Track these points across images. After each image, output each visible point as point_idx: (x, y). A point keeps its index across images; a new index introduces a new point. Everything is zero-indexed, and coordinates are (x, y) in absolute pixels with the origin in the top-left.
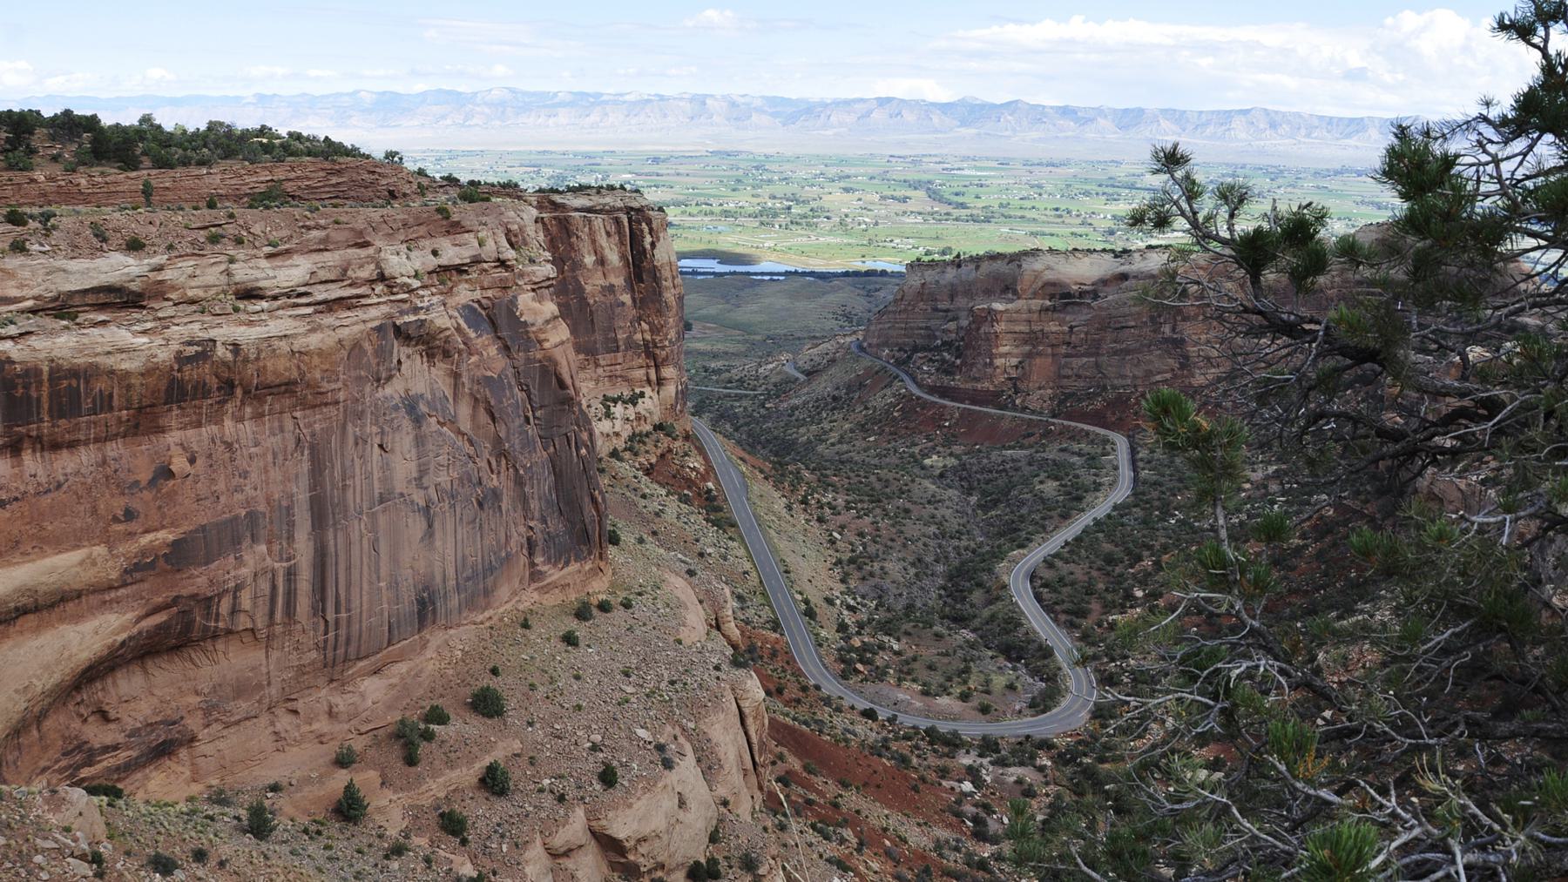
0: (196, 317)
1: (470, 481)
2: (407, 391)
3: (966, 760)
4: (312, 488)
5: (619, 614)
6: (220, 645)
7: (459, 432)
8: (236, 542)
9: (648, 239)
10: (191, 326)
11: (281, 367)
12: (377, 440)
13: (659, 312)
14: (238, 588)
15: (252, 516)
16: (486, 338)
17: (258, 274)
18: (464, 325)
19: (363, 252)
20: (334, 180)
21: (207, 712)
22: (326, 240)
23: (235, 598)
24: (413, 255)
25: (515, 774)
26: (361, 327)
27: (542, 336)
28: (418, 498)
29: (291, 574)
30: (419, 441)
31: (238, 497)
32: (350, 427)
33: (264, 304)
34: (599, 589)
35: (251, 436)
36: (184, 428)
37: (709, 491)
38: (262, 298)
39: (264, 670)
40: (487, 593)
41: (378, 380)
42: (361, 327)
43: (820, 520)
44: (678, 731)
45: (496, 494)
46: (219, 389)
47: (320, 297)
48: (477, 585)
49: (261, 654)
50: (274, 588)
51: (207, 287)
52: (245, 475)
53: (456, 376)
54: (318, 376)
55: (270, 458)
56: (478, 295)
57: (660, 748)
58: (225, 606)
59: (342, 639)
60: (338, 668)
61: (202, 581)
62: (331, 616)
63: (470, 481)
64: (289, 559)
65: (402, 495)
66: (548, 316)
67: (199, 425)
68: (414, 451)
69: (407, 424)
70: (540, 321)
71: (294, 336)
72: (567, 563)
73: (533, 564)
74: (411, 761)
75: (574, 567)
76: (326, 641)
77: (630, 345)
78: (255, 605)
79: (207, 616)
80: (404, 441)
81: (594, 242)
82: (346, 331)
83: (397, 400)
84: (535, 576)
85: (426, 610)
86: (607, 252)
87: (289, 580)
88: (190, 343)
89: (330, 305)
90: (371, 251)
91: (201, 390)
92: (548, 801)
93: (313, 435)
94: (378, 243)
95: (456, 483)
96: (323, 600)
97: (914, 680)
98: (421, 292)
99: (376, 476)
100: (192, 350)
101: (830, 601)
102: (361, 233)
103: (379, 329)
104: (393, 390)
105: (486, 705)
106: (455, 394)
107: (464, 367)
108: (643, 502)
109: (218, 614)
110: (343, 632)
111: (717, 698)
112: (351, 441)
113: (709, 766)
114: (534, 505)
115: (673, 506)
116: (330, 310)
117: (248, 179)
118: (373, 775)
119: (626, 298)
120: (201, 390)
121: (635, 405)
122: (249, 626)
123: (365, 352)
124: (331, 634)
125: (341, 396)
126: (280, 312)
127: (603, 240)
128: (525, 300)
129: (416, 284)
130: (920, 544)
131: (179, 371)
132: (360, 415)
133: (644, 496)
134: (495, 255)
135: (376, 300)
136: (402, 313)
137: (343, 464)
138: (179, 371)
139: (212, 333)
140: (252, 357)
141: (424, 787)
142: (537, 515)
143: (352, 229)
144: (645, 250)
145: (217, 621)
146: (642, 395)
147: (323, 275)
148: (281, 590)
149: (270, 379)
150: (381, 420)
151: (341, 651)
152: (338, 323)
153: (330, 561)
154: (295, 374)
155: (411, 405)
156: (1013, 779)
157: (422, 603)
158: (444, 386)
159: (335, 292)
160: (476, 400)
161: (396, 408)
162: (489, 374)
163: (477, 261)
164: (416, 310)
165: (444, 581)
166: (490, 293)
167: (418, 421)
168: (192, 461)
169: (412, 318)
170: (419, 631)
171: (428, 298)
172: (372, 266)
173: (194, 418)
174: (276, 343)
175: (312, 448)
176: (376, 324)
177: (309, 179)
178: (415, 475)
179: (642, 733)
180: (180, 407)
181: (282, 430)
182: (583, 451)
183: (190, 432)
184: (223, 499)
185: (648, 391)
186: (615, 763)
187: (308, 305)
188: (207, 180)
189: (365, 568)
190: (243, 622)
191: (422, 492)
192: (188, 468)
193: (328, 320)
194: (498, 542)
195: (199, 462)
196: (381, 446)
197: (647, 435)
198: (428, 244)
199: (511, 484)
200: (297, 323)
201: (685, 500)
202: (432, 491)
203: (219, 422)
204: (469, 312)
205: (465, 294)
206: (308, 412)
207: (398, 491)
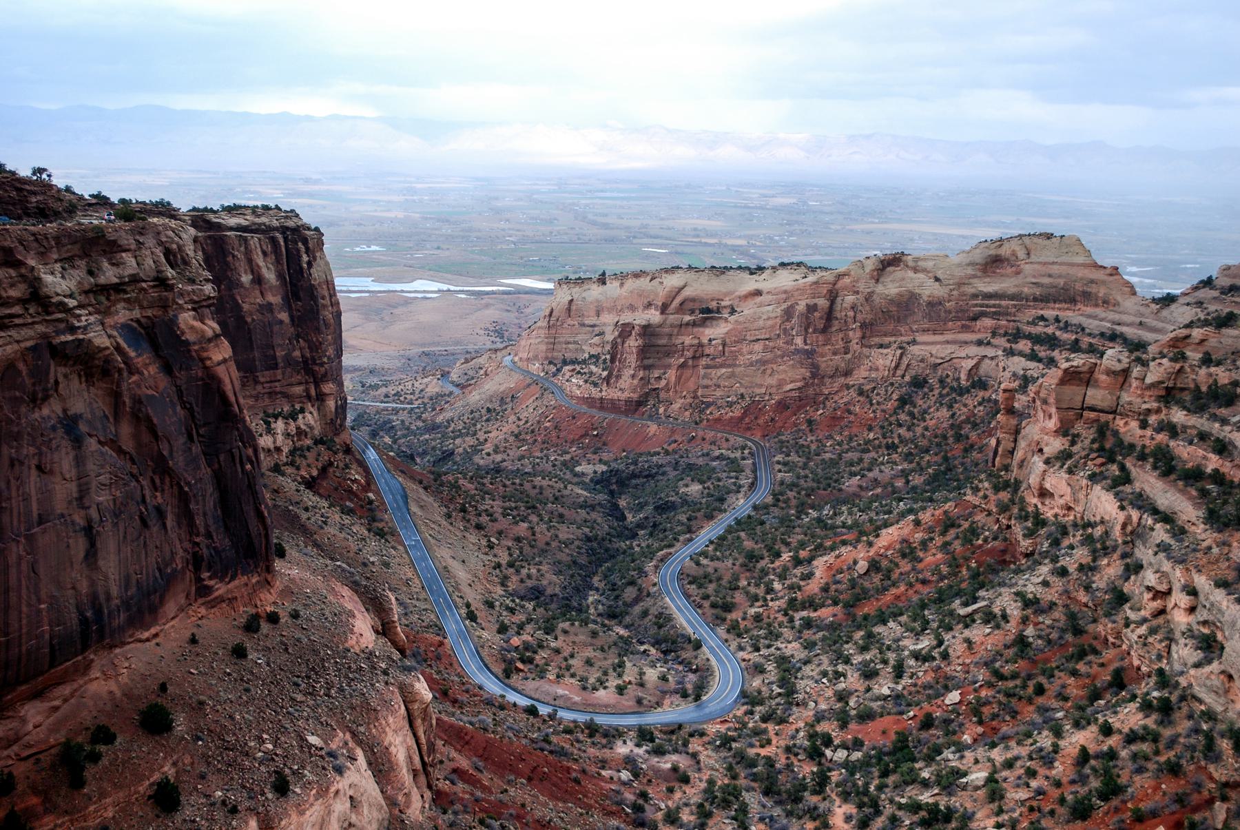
2: (65, 411)
3: (623, 749)
9: (305, 258)
12: (34, 462)
13: (318, 330)
26: (16, 347)
27: (205, 355)
30: (79, 461)
37: (371, 502)
42: (16, 347)
43: (479, 527)
44: (348, 736)
56: (137, 313)
57: (331, 754)
72: (233, 578)
73: (199, 580)
77: (289, 361)
80: (64, 461)
81: (250, 261)
86: (264, 271)
97: (573, 676)
98: (78, 312)
99: (34, 499)
103: (33, 349)
104: (50, 411)
107: (124, 386)
111: (387, 703)
113: (381, 768)
114: (199, 521)
115: (335, 516)
119: (284, 316)
121: (295, 420)
123: (20, 372)
130: (572, 547)
133: (307, 509)
134: (154, 274)
135: (30, 321)
136: (58, 333)
142: (202, 530)
144: (301, 268)
146: (302, 411)
150: (39, 440)
156: (669, 766)
157: (84, 621)
158: (102, 406)
161: (54, 428)
166: (149, 313)
167: (77, 442)
169: (70, 338)
171: (86, 318)
176: (29, 344)
178: (75, 495)
179: (313, 740)
186: (287, 771)
191: (83, 512)
196: (39, 468)
197: (309, 449)
202: (94, 513)
205: (123, 315)
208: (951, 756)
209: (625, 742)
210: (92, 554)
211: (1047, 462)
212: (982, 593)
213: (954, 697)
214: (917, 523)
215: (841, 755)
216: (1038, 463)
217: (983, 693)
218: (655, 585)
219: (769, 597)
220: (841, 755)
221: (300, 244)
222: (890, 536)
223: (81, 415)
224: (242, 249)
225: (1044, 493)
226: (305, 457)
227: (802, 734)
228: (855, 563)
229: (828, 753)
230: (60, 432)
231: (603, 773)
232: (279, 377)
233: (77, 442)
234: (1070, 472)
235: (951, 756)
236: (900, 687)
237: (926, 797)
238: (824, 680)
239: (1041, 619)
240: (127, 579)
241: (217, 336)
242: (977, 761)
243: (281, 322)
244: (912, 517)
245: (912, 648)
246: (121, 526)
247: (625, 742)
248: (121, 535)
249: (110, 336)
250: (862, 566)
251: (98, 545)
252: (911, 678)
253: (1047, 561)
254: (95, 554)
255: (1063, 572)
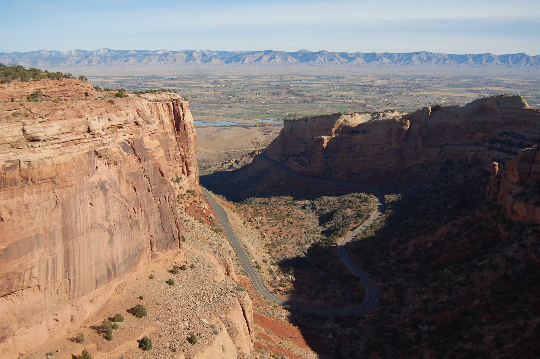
0: (12, 150)
1: (127, 217)
2: (100, 180)
3: (329, 325)
4: (63, 223)
5: (189, 271)
6: (24, 292)
7: (121, 196)
8: (31, 248)
9: (181, 113)
10: (8, 154)
11: (48, 171)
12: (89, 201)
13: (187, 143)
14: (32, 268)
15: (37, 236)
16: (132, 156)
17: (37, 130)
18: (122, 151)
19: (80, 120)
20: (62, 89)
21: (19, 323)
22: (64, 115)
23: (31, 272)
24: (100, 120)
25: (154, 342)
26: (81, 152)
27: (154, 154)
28: (106, 225)
29: (54, 261)
30: (106, 201)
31: (31, 228)
32: (78, 197)
33: (41, 144)
34: (180, 261)
35: (36, 201)
36: (7, 199)
37: (211, 218)
38: (39, 141)
39: (43, 303)
40: (135, 264)
41: (89, 175)
42: (81, 152)
43: (257, 228)
44: (219, 319)
45: (137, 222)
46: (22, 181)
47: (64, 140)
48: (131, 262)
49: (42, 296)
50: (48, 267)
51: (14, 137)
52: (33, 218)
53: (120, 172)
54: (64, 174)
55: (44, 210)
56: (127, 137)
57: (212, 327)
58: (27, 276)
59: (77, 288)
60: (75, 299)
61: (17, 265)
62: (72, 278)
63: (127, 217)
64: (54, 254)
65: (100, 224)
66: (156, 146)
67: (13, 197)
68: (104, 205)
69: (101, 194)
70: (153, 148)
71: (54, 157)
72: (166, 250)
73: (152, 251)
74: (108, 338)
75: (169, 252)
76: (70, 289)
77: (175, 158)
78: (40, 275)
79: (19, 281)
80: (99, 201)
81: (159, 114)
82: (75, 154)
83: (97, 183)
84: (154, 256)
85: (111, 272)
86: (164, 118)
87: (54, 263)
88: (8, 162)
89: (66, 143)
90: (83, 119)
91: (14, 182)
92: (169, 352)
93: (63, 200)
94: (87, 116)
95: (121, 218)
96: (68, 271)
97: (304, 293)
98: (105, 137)
99: (89, 217)
100: (9, 165)
101: (265, 261)
102: (79, 112)
103: (89, 153)
104: (95, 179)
105: (137, 312)
106: (119, 181)
107: (123, 168)
108: (185, 223)
109: (24, 280)
110: (77, 284)
111: (233, 304)
112: (78, 202)
113: (232, 333)
114: (152, 226)
115: (197, 224)
116: (68, 145)
117: (26, 89)
118: (93, 345)
119: (173, 138)
120: (14, 182)
121: (178, 182)
122: (37, 284)
123: (83, 163)
124: (72, 286)
125: (74, 182)
126: (47, 147)
127: (162, 113)
128: (146, 139)
129: (103, 133)
130: (299, 236)
131: (4, 174)
132: (82, 191)
133: (185, 221)
134: (134, 120)
135: (87, 141)
136: (98, 146)
137: (75, 212)
138: (4, 174)
139: (19, 157)
140: (36, 167)
141: (116, 349)
142: (154, 231)
143: (76, 110)
144: (180, 117)
145: (23, 282)
146: (181, 178)
147: (64, 130)
148: (50, 268)
149: (44, 176)
150: (90, 192)
151: (76, 293)
152: (71, 151)
153: (71, 254)
154: (54, 174)
155: (102, 186)
156: (349, 332)
157: (109, 270)
158: (115, 177)
159: (70, 137)
160: (128, 182)
161: (96, 187)
162: (133, 171)
163: (126, 122)
164: (104, 144)
165: (118, 261)
166: (132, 136)
167: (105, 191)
168: (11, 213)
169: (102, 148)
170: (108, 282)
171: (108, 139)
172: (84, 126)
173: (11, 194)
174: (46, 160)
175: (62, 205)
176: (87, 151)
177: (51, 88)
178: (105, 215)
179: (204, 321)
180: (4, 190)
181: (49, 198)
182: (172, 203)
183: (9, 201)
184: (25, 229)
185: (183, 176)
186: (195, 334)
187: (59, 143)
188: (8, 89)
189: (86, 256)
190: (34, 282)
191: (108, 223)
192: (9, 217)
193: (67, 150)
194: (139, 243)
195: (14, 213)
196: (91, 204)
197: (184, 195)
198: (106, 116)
199: (143, 218)
200: (55, 151)
201: (201, 221)
202: (112, 222)
203: (22, 196)
204: (124, 145)
205: (122, 136)
206: (60, 190)
207: (98, 222)
208: (477, 328)
209: (329, 322)
210: (111, 241)
211: (514, 197)
212: (486, 256)
213: (476, 302)
214: (454, 225)
215: (426, 328)
216: (510, 198)
217: (490, 301)
218: (336, 253)
219: (388, 258)
220: (426, 328)
221: (179, 106)
222: (442, 230)
223: (106, 181)
224: (155, 109)
225: (513, 211)
226: (183, 198)
227: (408, 319)
228: (427, 242)
229: (420, 327)
230: (99, 189)
231: (321, 335)
232: (171, 164)
233: (105, 191)
234: (526, 201)
235: (477, 328)
236: (451, 298)
237: (467, 346)
238: (416, 295)
239: (514, 267)
240: (125, 250)
241: (159, 146)
242: (489, 331)
243: (172, 140)
244: (452, 222)
245: (456, 280)
246: (123, 229)
247: (329, 322)
248: (123, 232)
249: (117, 147)
250: (430, 245)
251: (114, 236)
252: (456, 293)
253: (516, 241)
254: (112, 241)
255: (524, 246)
